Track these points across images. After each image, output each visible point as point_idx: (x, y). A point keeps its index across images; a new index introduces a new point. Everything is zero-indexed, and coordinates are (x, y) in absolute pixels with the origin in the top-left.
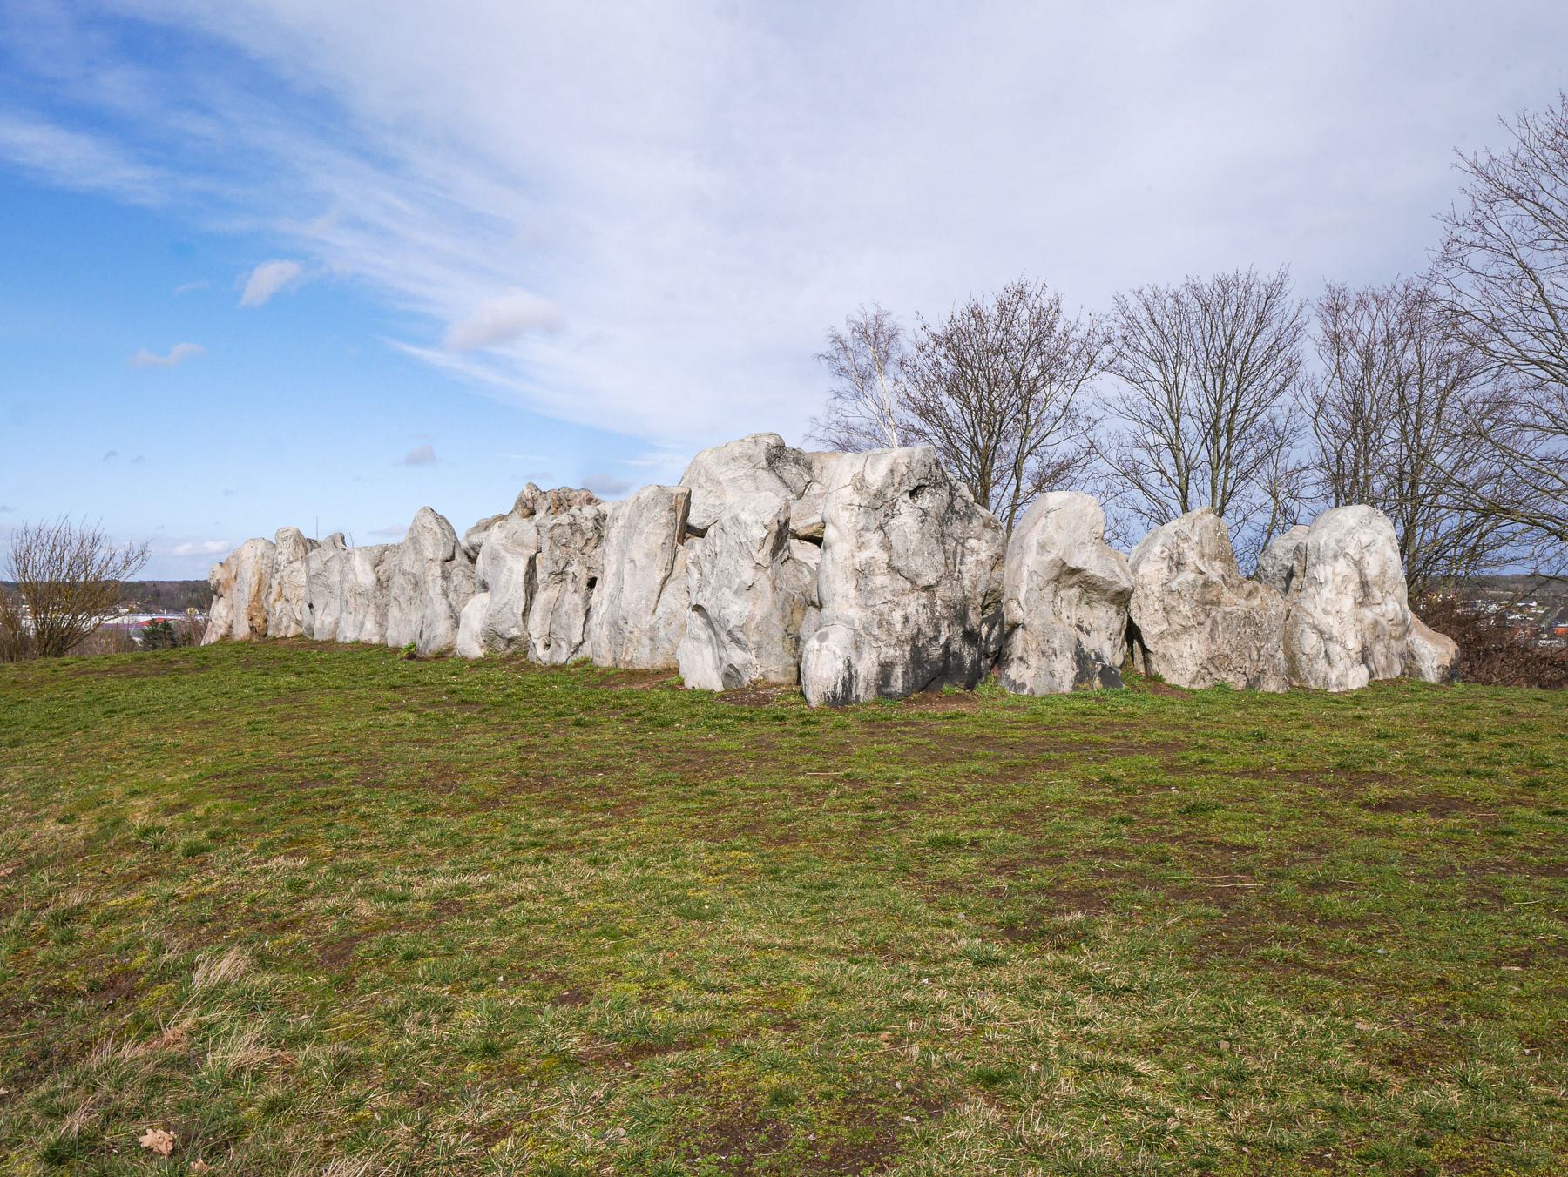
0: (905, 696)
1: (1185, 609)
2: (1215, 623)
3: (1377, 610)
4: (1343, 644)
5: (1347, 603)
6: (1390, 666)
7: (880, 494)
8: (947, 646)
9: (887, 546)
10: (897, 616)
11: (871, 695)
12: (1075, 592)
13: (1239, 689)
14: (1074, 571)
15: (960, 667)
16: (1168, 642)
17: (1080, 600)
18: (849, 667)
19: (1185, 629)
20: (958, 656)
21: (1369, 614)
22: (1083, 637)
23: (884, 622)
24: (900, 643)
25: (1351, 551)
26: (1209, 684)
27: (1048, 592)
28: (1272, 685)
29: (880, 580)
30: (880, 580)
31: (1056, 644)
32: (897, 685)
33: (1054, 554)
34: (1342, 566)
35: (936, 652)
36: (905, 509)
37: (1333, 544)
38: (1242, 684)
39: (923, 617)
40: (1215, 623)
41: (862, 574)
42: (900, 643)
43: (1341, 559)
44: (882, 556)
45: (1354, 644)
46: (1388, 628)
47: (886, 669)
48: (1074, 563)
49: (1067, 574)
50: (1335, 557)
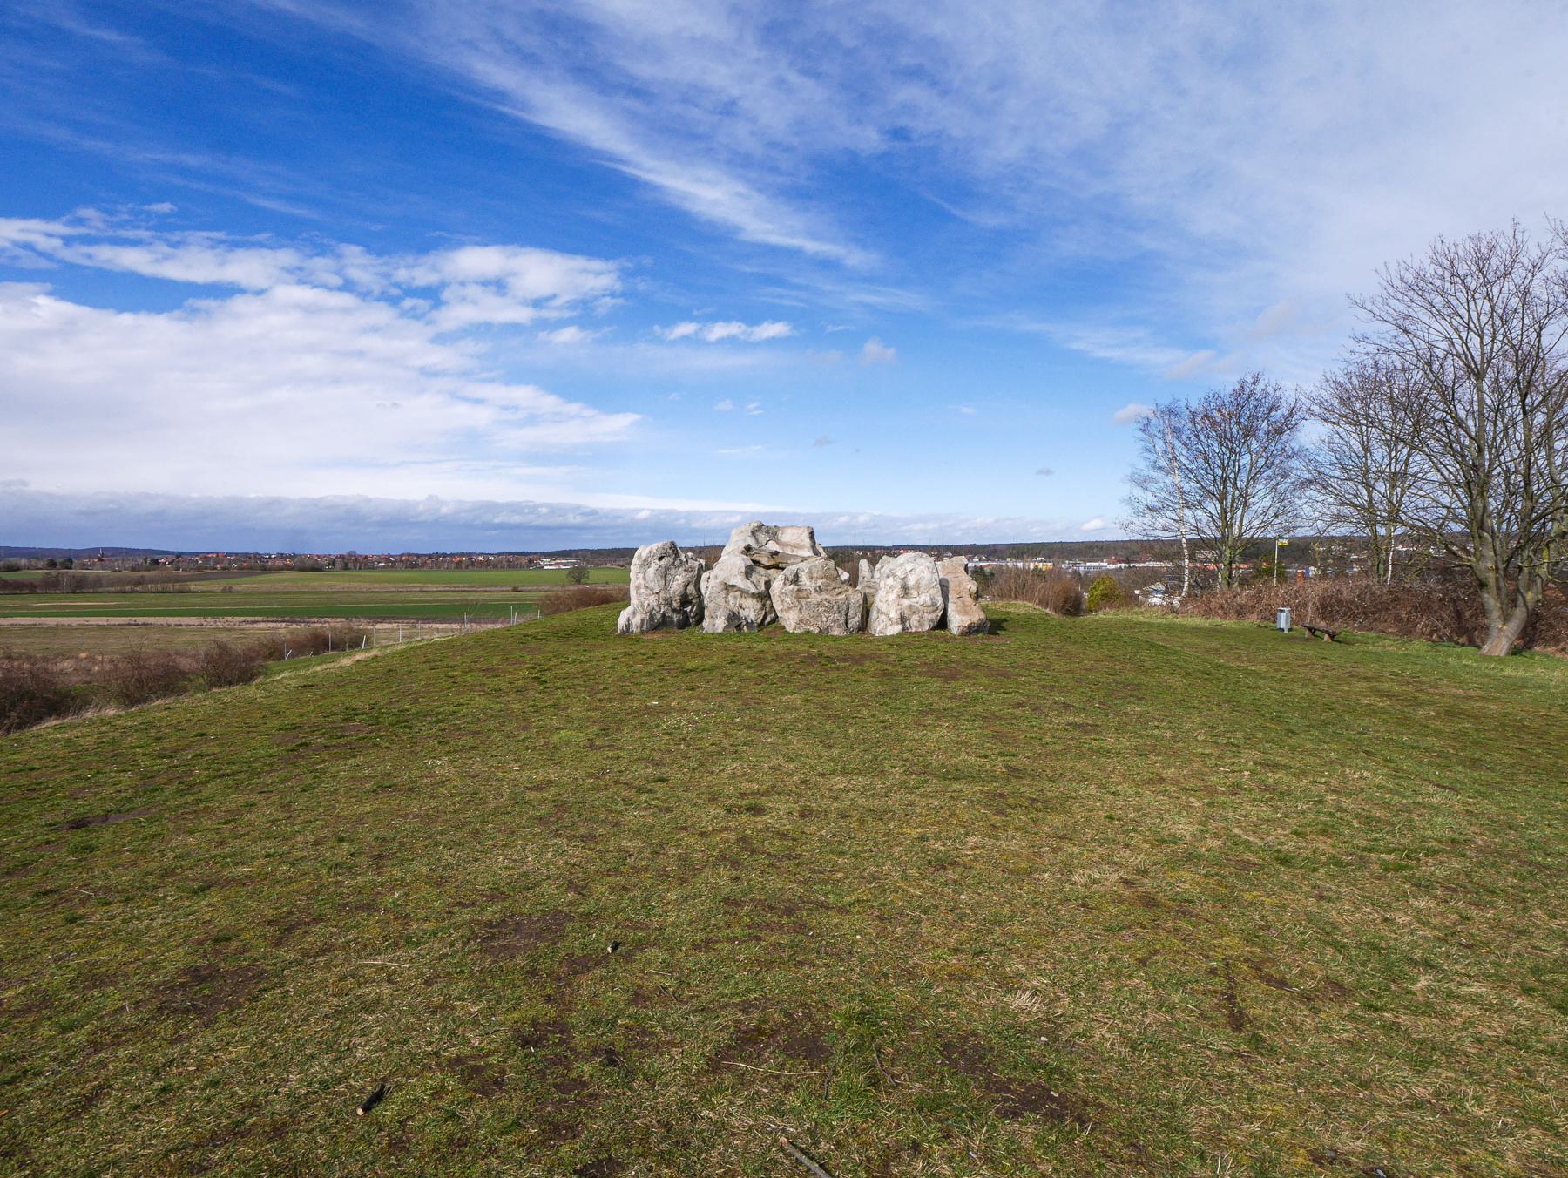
0: (647, 631)
1: (789, 600)
2: (802, 606)
3: (914, 600)
4: (888, 616)
5: (892, 597)
6: (921, 625)
7: (645, 560)
8: (664, 615)
9: (645, 579)
10: (646, 603)
11: (639, 630)
12: (738, 593)
13: (720, 630)
14: (734, 586)
15: (672, 622)
16: (784, 613)
17: (741, 596)
18: (629, 620)
19: (790, 608)
20: (671, 617)
21: (906, 602)
22: (741, 611)
23: (642, 605)
24: (646, 613)
25: (899, 574)
26: (802, 630)
27: (723, 594)
28: (836, 632)
29: (642, 590)
30: (642, 590)
31: (718, 614)
32: (645, 628)
33: (720, 579)
34: (890, 581)
35: (659, 616)
36: (653, 565)
37: (887, 571)
38: (817, 631)
39: (655, 603)
40: (802, 606)
41: (638, 588)
42: (646, 613)
43: (891, 578)
44: (643, 582)
45: (894, 615)
46: (921, 608)
47: (642, 621)
48: (731, 582)
49: (728, 588)
50: (888, 577)
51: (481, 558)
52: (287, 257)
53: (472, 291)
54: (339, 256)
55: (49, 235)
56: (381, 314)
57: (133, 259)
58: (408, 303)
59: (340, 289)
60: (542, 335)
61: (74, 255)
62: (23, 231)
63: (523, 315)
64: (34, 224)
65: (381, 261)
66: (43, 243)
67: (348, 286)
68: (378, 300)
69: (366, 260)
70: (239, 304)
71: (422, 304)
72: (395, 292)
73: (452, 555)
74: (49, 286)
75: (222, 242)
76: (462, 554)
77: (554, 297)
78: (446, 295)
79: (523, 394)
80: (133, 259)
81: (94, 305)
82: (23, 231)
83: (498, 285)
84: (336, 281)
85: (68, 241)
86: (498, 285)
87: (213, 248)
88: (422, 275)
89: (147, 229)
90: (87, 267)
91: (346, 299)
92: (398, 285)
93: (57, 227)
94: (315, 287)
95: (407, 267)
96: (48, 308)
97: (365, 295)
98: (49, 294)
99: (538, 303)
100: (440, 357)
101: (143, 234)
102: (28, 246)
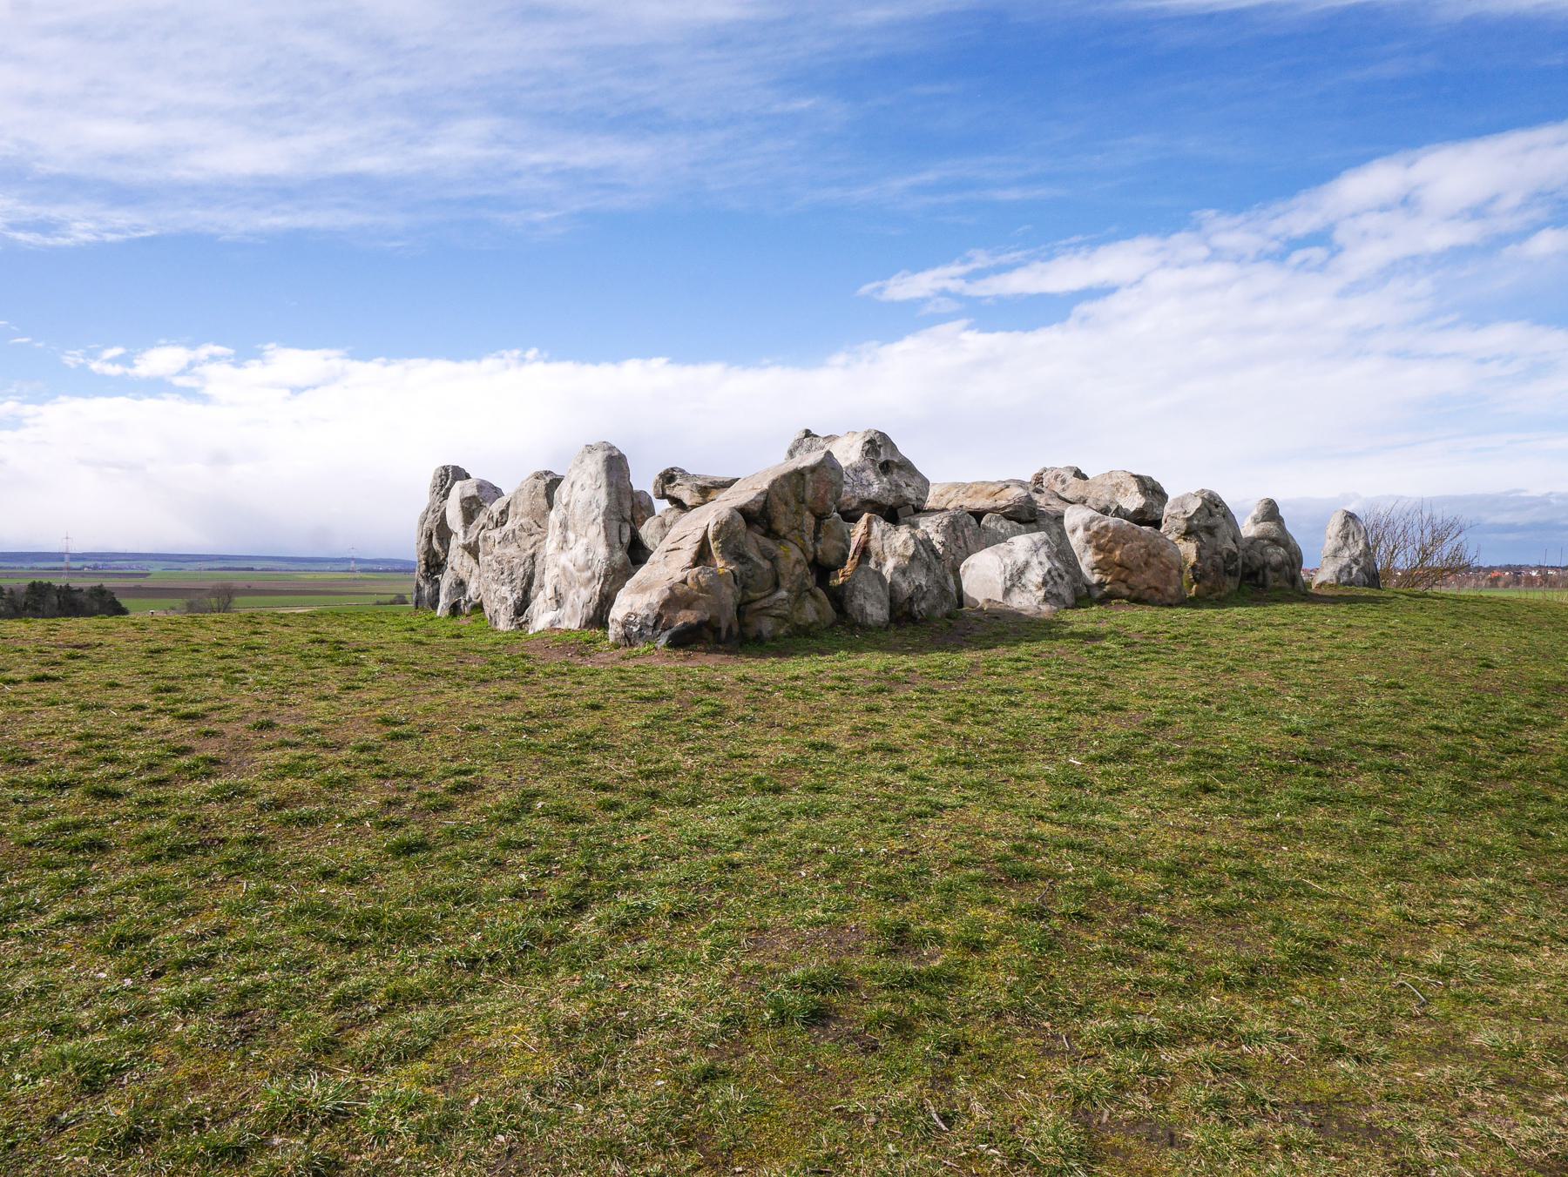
51: (1534, 574)
52: (1145, 244)
53: (1371, 222)
54: (1197, 228)
55: (953, 278)
56: (1267, 278)
57: (1022, 282)
58: (1297, 257)
59: (1208, 260)
60: (1510, 251)
61: (980, 289)
62: (935, 279)
63: (1467, 233)
64: (939, 272)
65: (1241, 218)
66: (953, 286)
67: (1216, 255)
68: (1256, 260)
69: (1223, 222)
70: (1115, 304)
71: (1317, 253)
72: (1274, 246)
73: (1491, 569)
74: (963, 322)
75: (1079, 245)
76: (1508, 568)
77: (1494, 199)
78: (1340, 236)
79: (1502, 336)
80: (1022, 282)
81: (1009, 329)
82: (935, 279)
83: (1407, 203)
84: (1203, 252)
85: (969, 277)
86: (1407, 203)
87: (1076, 253)
88: (1299, 218)
89: (1018, 250)
90: (985, 298)
91: (1215, 272)
92: (1275, 238)
93: (956, 270)
94: (1182, 267)
95: (1277, 216)
96: (977, 342)
97: (1239, 259)
98: (969, 328)
99: (1477, 212)
100: (1361, 311)
101: (1018, 255)
102: (944, 293)
